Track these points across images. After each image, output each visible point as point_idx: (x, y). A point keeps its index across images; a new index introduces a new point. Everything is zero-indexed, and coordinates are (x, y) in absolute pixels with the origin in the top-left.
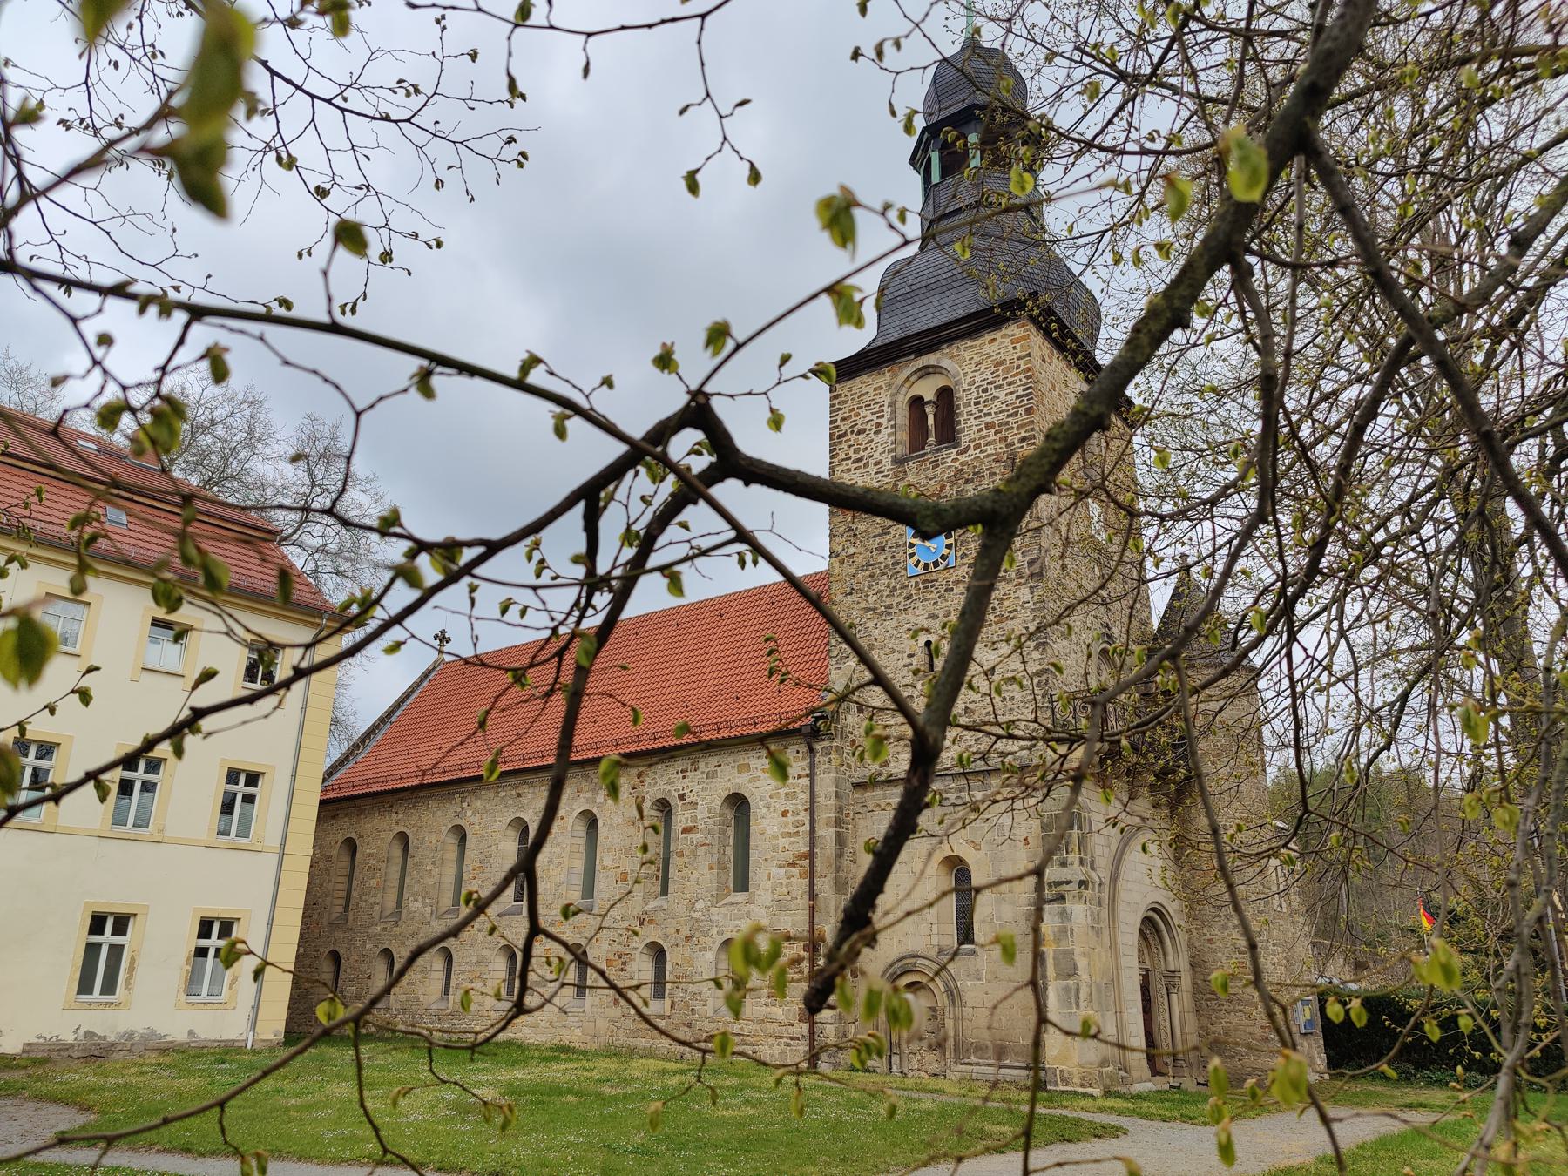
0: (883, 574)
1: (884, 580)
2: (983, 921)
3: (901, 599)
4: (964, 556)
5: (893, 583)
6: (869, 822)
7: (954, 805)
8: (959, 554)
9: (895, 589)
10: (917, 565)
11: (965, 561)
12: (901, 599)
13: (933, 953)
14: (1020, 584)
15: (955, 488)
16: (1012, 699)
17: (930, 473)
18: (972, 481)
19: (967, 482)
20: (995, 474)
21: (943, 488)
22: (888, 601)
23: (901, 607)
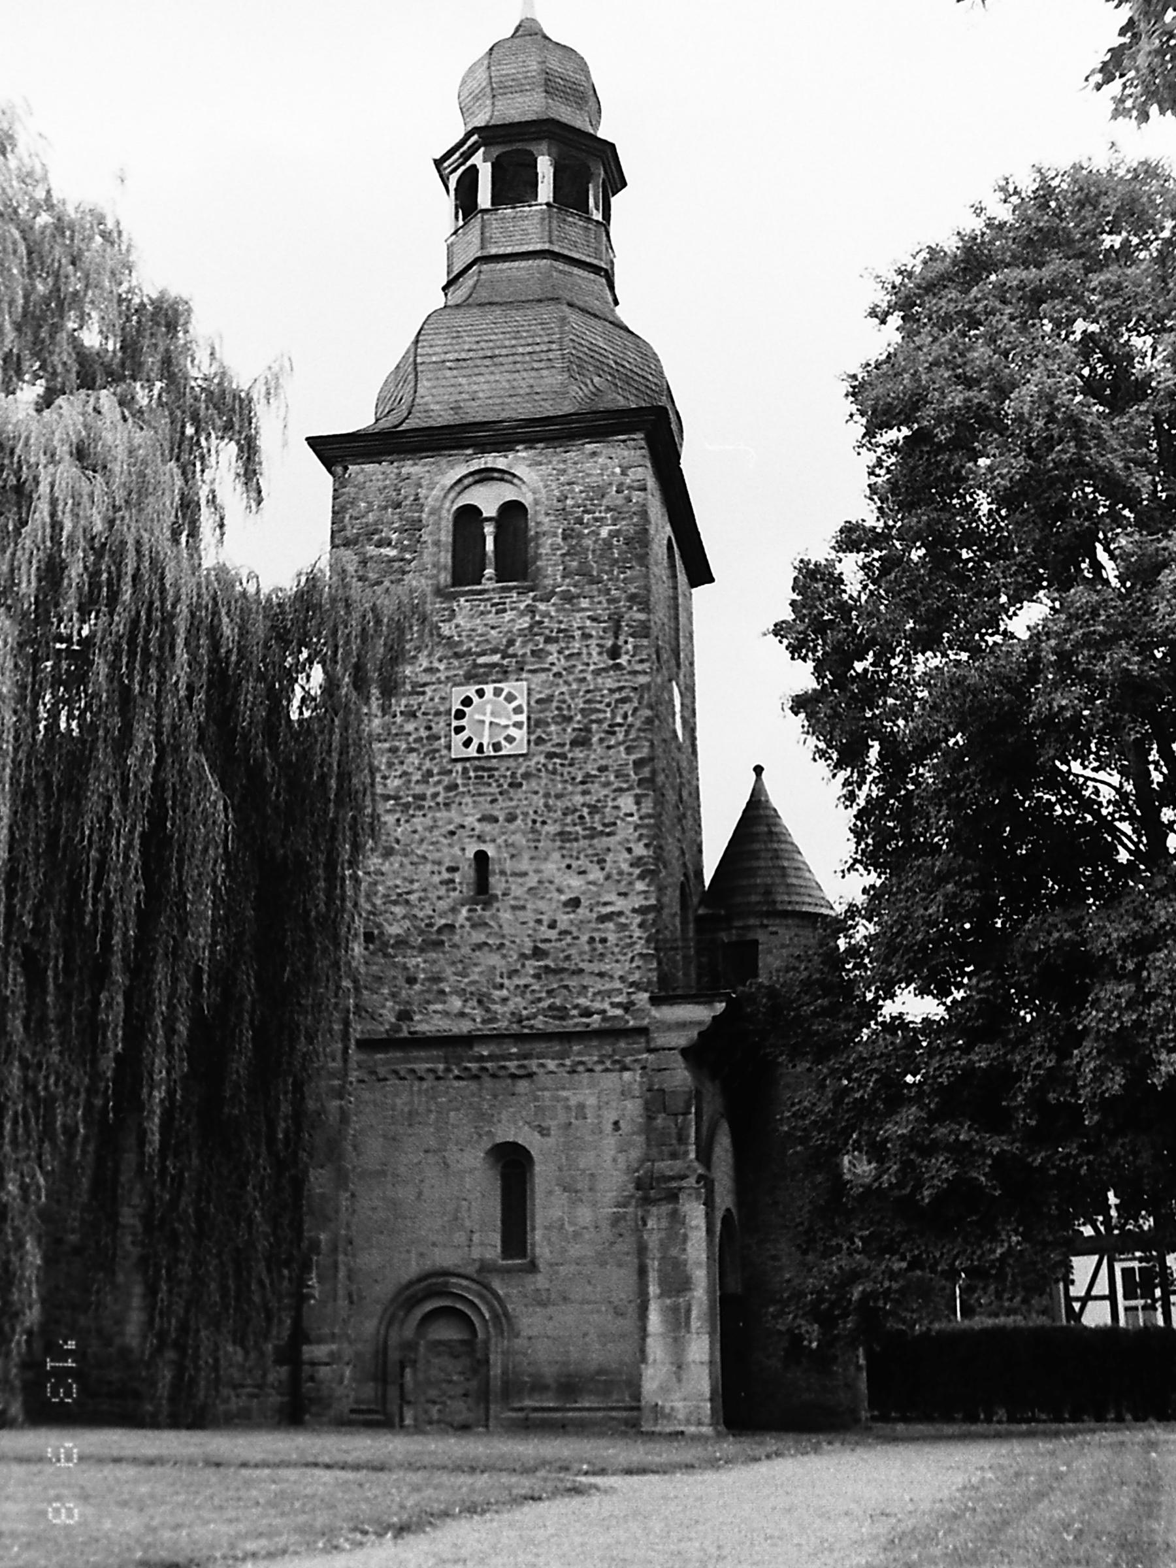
0: (411, 750)
1: (413, 758)
3: (440, 788)
4: (540, 741)
5: (428, 764)
7: (514, 1077)
8: (533, 737)
9: (430, 773)
10: (467, 743)
11: (541, 748)
12: (440, 788)
13: (471, 1270)
14: (621, 790)
15: (530, 646)
16: (604, 941)
17: (491, 619)
18: (556, 640)
19: (548, 640)
20: (590, 636)
21: (511, 643)
22: (419, 789)
23: (440, 799)
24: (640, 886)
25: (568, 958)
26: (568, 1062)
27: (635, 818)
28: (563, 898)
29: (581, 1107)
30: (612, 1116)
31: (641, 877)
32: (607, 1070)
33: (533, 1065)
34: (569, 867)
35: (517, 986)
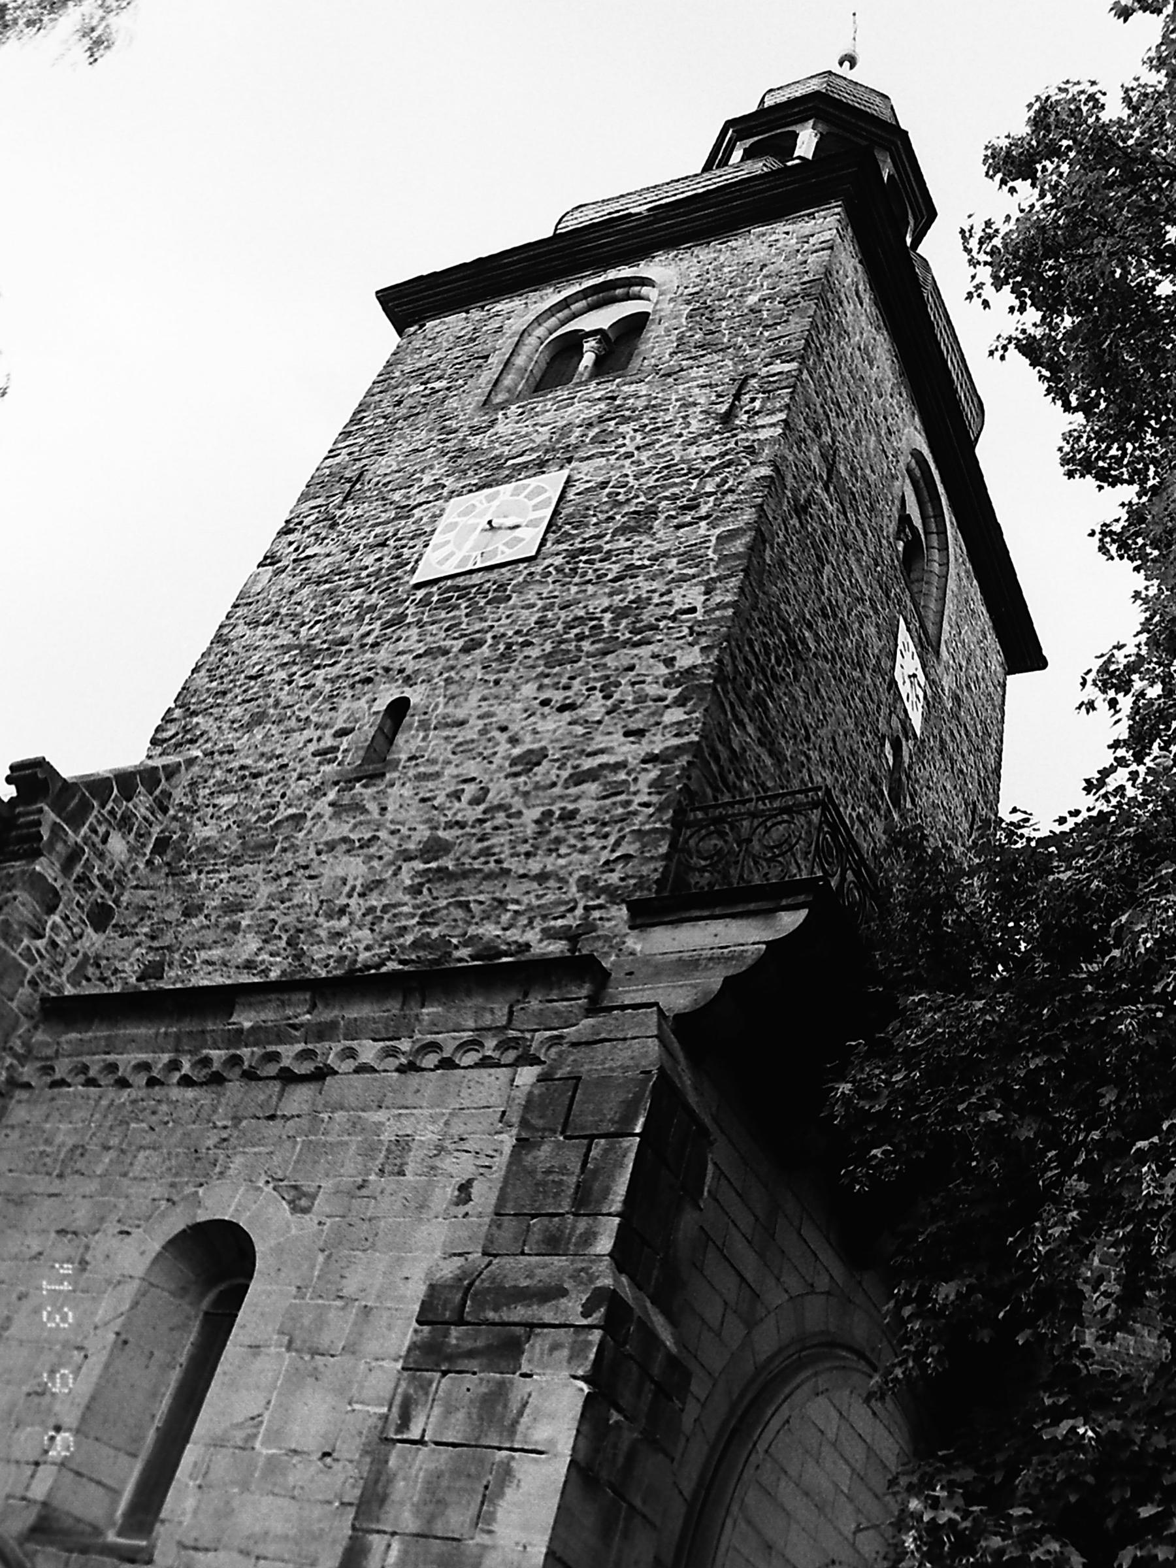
2: (218, 1443)
6: (38, 1112)
14: (684, 578)
24: (676, 715)
25: (487, 852)
26: (405, 1045)
27: (699, 615)
28: (517, 751)
29: (402, 1144)
30: (459, 1167)
31: (680, 702)
32: (485, 1063)
33: (331, 1052)
34: (545, 703)
35: (371, 910)
